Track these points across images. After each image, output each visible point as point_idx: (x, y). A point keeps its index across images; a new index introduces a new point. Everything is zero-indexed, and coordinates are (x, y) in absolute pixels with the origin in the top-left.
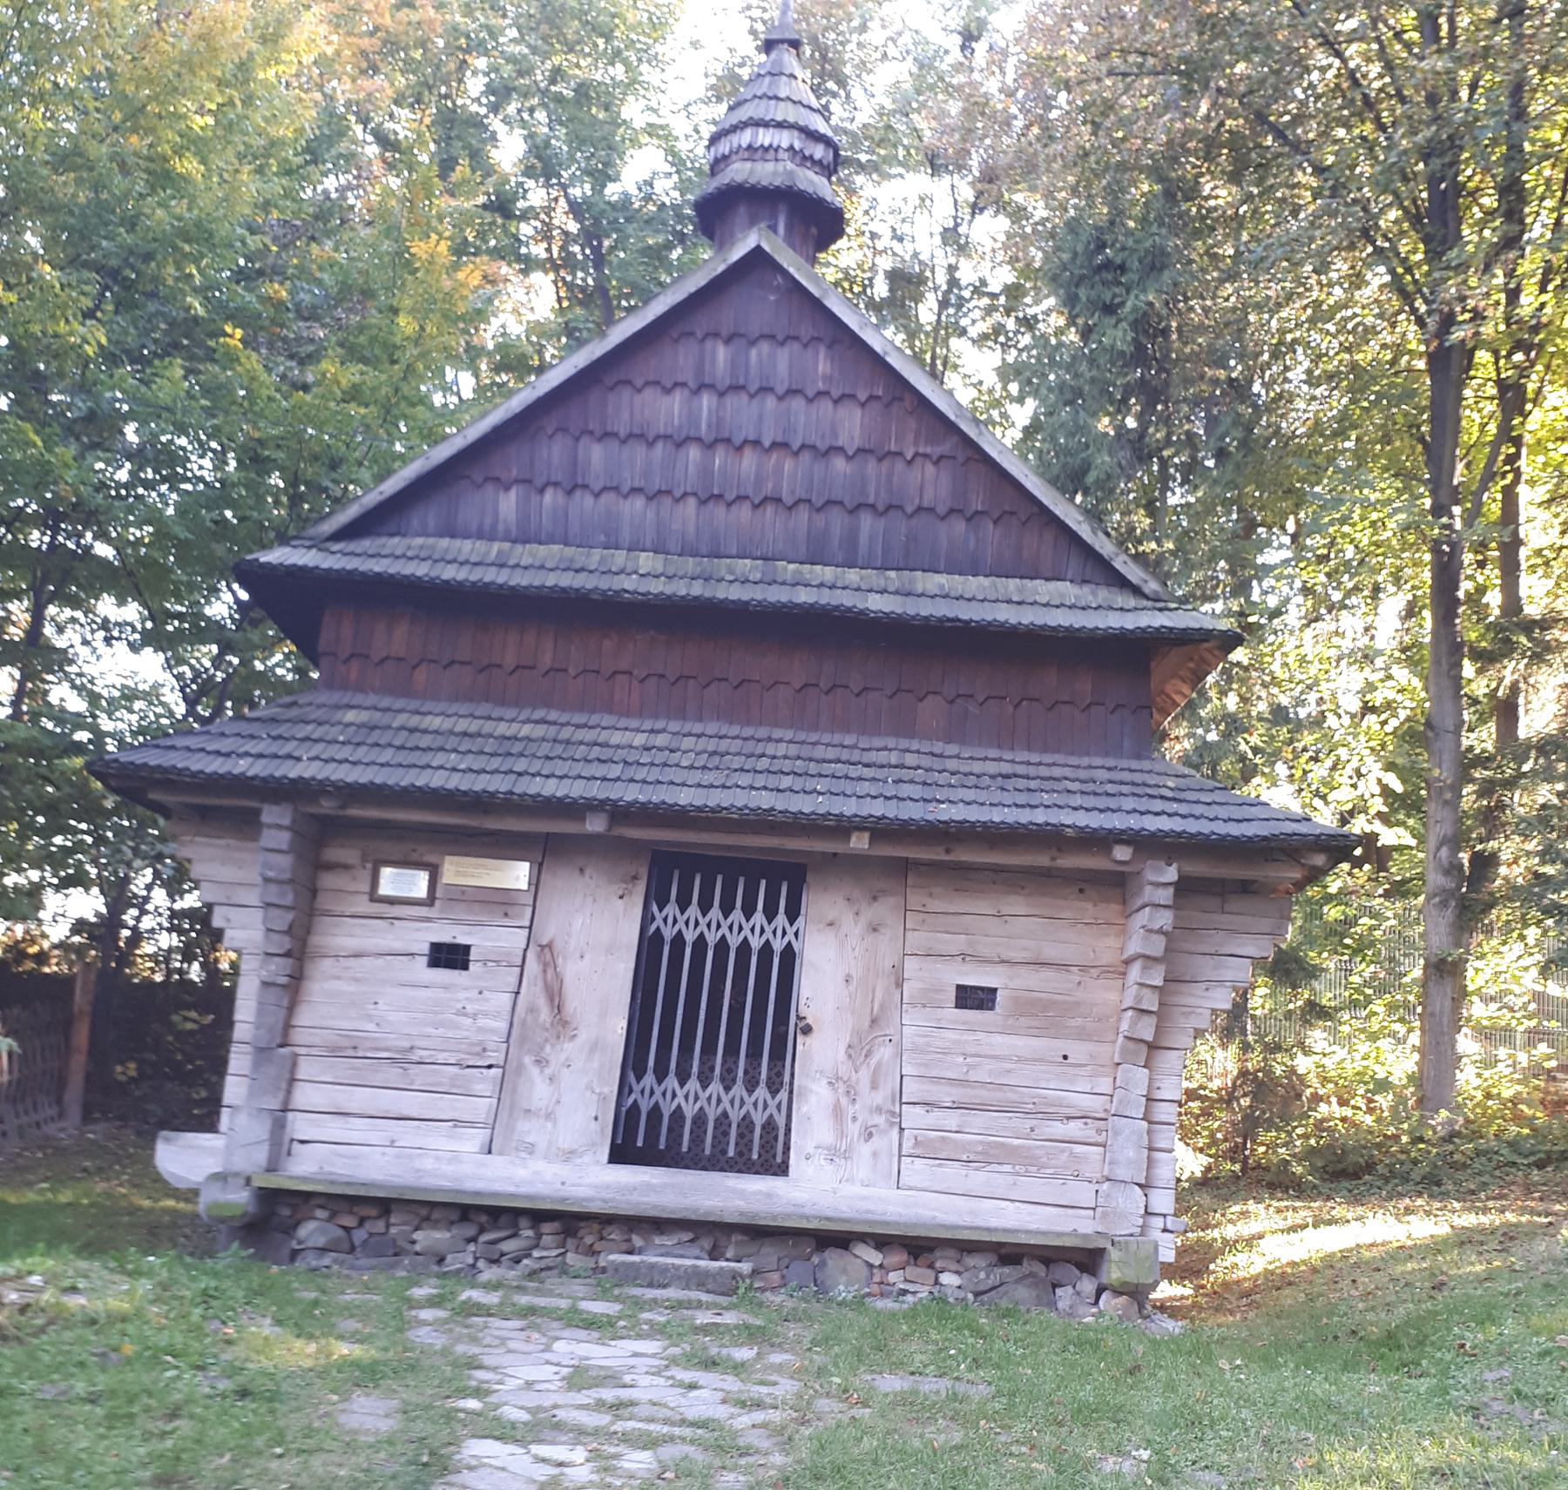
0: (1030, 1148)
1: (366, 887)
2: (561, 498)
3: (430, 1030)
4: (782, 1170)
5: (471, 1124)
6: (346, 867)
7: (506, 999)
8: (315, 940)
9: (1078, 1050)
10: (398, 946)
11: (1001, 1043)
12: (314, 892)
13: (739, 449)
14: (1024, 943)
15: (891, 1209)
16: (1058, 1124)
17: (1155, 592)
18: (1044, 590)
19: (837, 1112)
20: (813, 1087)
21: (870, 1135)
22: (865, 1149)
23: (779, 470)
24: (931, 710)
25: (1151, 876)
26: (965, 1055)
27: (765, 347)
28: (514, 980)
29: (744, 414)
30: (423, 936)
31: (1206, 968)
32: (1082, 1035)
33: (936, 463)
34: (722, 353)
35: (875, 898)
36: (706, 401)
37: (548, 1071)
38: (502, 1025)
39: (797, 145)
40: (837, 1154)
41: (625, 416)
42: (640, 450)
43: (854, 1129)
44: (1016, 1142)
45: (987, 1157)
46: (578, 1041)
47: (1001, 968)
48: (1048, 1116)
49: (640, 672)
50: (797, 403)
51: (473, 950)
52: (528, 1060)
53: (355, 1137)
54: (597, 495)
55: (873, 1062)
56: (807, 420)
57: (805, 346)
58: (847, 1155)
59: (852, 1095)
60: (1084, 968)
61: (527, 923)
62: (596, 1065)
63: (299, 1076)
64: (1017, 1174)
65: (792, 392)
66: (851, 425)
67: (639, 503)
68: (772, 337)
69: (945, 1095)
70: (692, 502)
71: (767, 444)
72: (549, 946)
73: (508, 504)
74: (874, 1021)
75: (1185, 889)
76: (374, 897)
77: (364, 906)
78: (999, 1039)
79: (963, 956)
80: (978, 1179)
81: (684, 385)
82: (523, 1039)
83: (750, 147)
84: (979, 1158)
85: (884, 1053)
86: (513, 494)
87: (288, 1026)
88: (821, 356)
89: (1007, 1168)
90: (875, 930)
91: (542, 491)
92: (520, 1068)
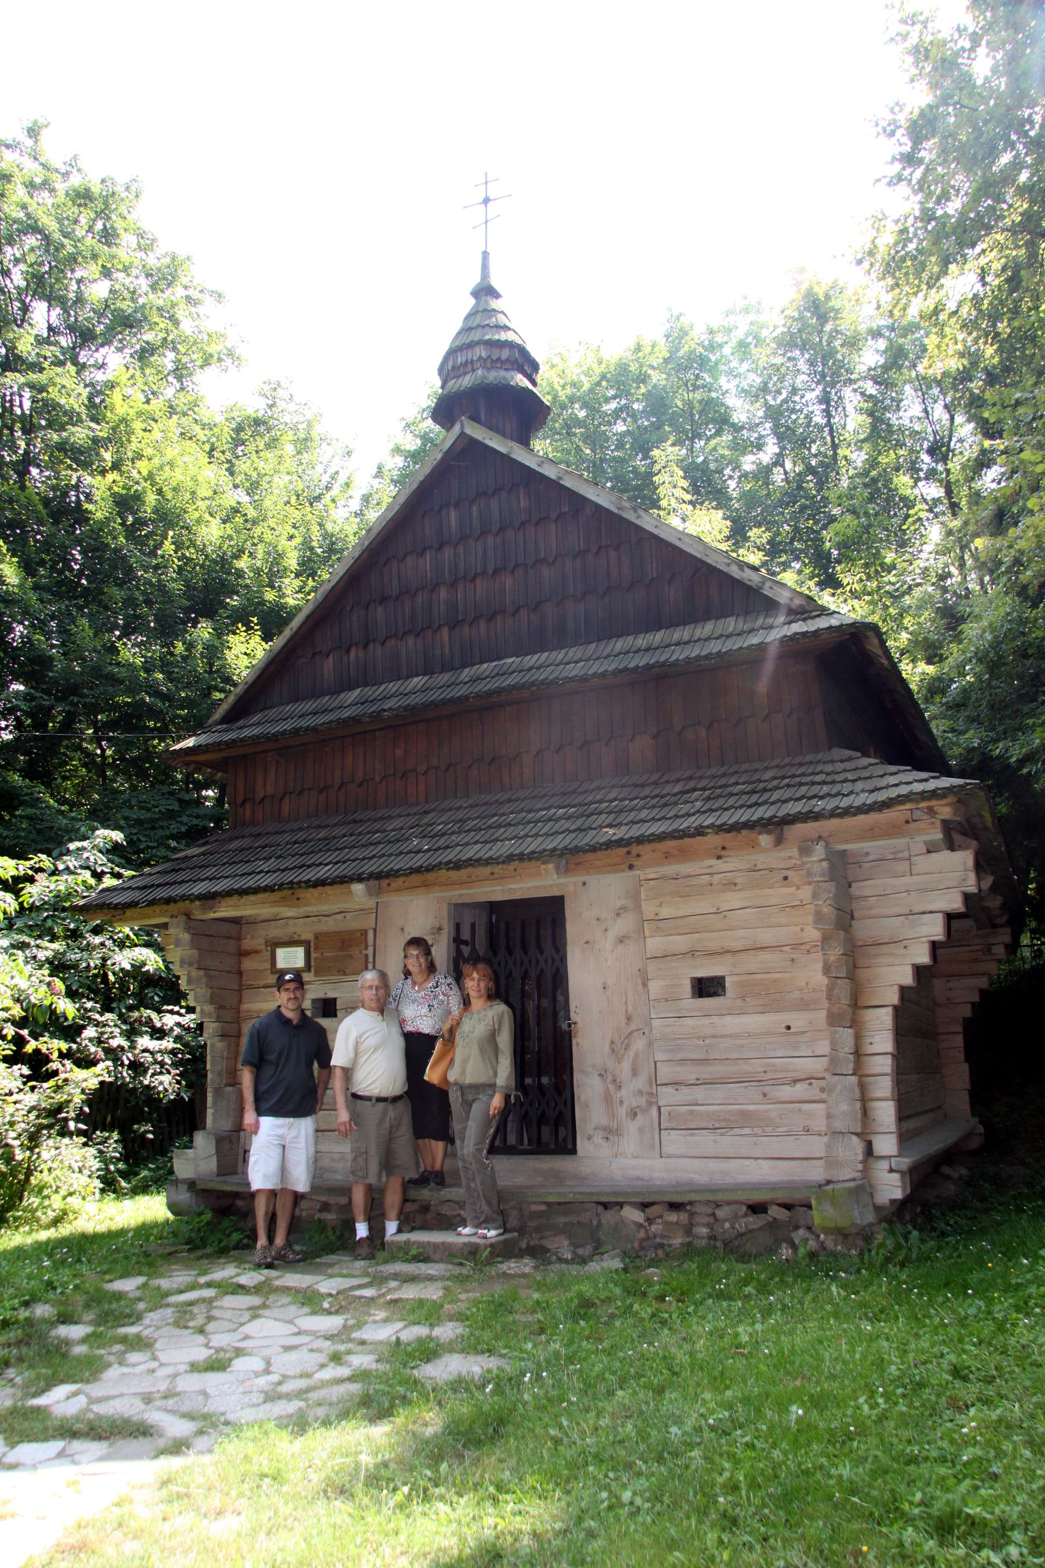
0: (766, 1111)
2: (361, 654)
8: (245, 1007)
9: (798, 1020)
11: (734, 1023)
12: (240, 973)
13: (473, 580)
14: (742, 933)
15: (656, 1174)
16: (787, 1087)
17: (801, 606)
19: (608, 1098)
21: (635, 1114)
22: (632, 1127)
26: (704, 1038)
32: (803, 1006)
33: (617, 548)
35: (618, 915)
39: (484, 355)
41: (395, 582)
43: (622, 1111)
44: (751, 1107)
45: (721, 1125)
47: (728, 958)
49: (421, 769)
51: (338, 1002)
54: (383, 644)
55: (632, 1053)
57: (510, 492)
60: (796, 946)
64: (756, 1135)
69: (690, 1073)
70: (445, 631)
73: (328, 666)
79: (692, 953)
80: (727, 1143)
81: (430, 547)
83: (453, 368)
84: (723, 1124)
85: (639, 1044)
86: (331, 658)
88: (521, 496)
89: (747, 1131)
90: (621, 941)
91: (348, 651)
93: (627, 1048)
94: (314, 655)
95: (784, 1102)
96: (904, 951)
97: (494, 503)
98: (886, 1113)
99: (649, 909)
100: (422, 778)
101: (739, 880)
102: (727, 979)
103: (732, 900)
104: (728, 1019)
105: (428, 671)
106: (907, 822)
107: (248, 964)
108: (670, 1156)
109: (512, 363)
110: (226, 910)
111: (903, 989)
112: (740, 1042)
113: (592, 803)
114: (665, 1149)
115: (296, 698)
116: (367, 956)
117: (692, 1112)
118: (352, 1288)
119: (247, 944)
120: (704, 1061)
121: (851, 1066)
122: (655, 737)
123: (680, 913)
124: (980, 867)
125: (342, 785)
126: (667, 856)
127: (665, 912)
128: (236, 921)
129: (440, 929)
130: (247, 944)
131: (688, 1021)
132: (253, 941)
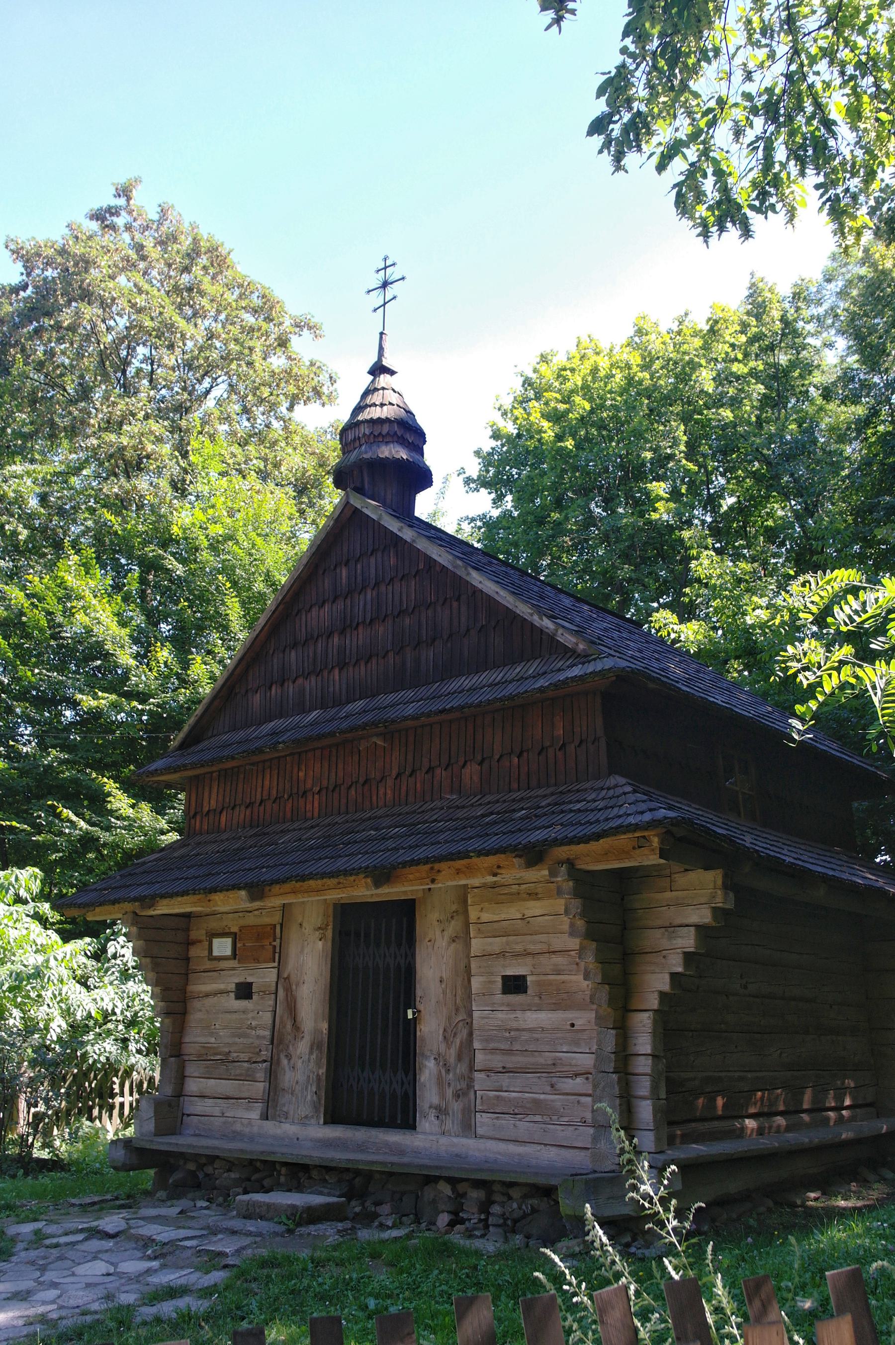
0: (553, 1101)
1: (206, 953)
3: (237, 1040)
4: (413, 1127)
5: (255, 1100)
6: (200, 941)
7: (267, 1017)
8: (191, 988)
12: (188, 959)
13: (357, 628)
16: (570, 1080)
20: (427, 1063)
21: (459, 1096)
26: (510, 1031)
28: (272, 1003)
30: (230, 982)
36: (340, 605)
37: (292, 1062)
38: (267, 1033)
39: (367, 432)
40: (441, 1112)
43: (449, 1092)
44: (542, 1097)
46: (304, 1040)
47: (529, 960)
52: (282, 1056)
53: (208, 1110)
54: (294, 682)
57: (383, 551)
61: (276, 964)
62: (314, 1056)
63: (187, 1074)
70: (336, 671)
71: (368, 621)
72: (288, 978)
76: (211, 958)
77: (208, 965)
79: (502, 954)
80: (523, 1127)
82: (281, 1041)
87: (180, 1043)
89: (538, 1118)
91: (270, 688)
92: (279, 1062)
93: (455, 1034)
94: (247, 691)
95: (567, 1094)
96: (663, 961)
98: (645, 1111)
99: (473, 914)
100: (316, 797)
101: (539, 890)
102: (529, 979)
103: (534, 908)
104: (528, 1013)
105: (323, 706)
106: (634, 848)
107: (195, 952)
108: (482, 1137)
109: (392, 436)
110: (164, 908)
111: (663, 995)
112: (536, 1036)
113: (419, 823)
114: (480, 1131)
115: (234, 729)
116: (275, 947)
117: (498, 1097)
118: (180, 1240)
119: (194, 935)
120: (509, 1052)
121: (612, 1065)
122: (481, 764)
123: (496, 918)
124: (729, 885)
125: (262, 801)
126: (458, 871)
127: (486, 917)
128: (188, 916)
129: (327, 925)
130: (194, 935)
131: (500, 1015)
132: (197, 933)
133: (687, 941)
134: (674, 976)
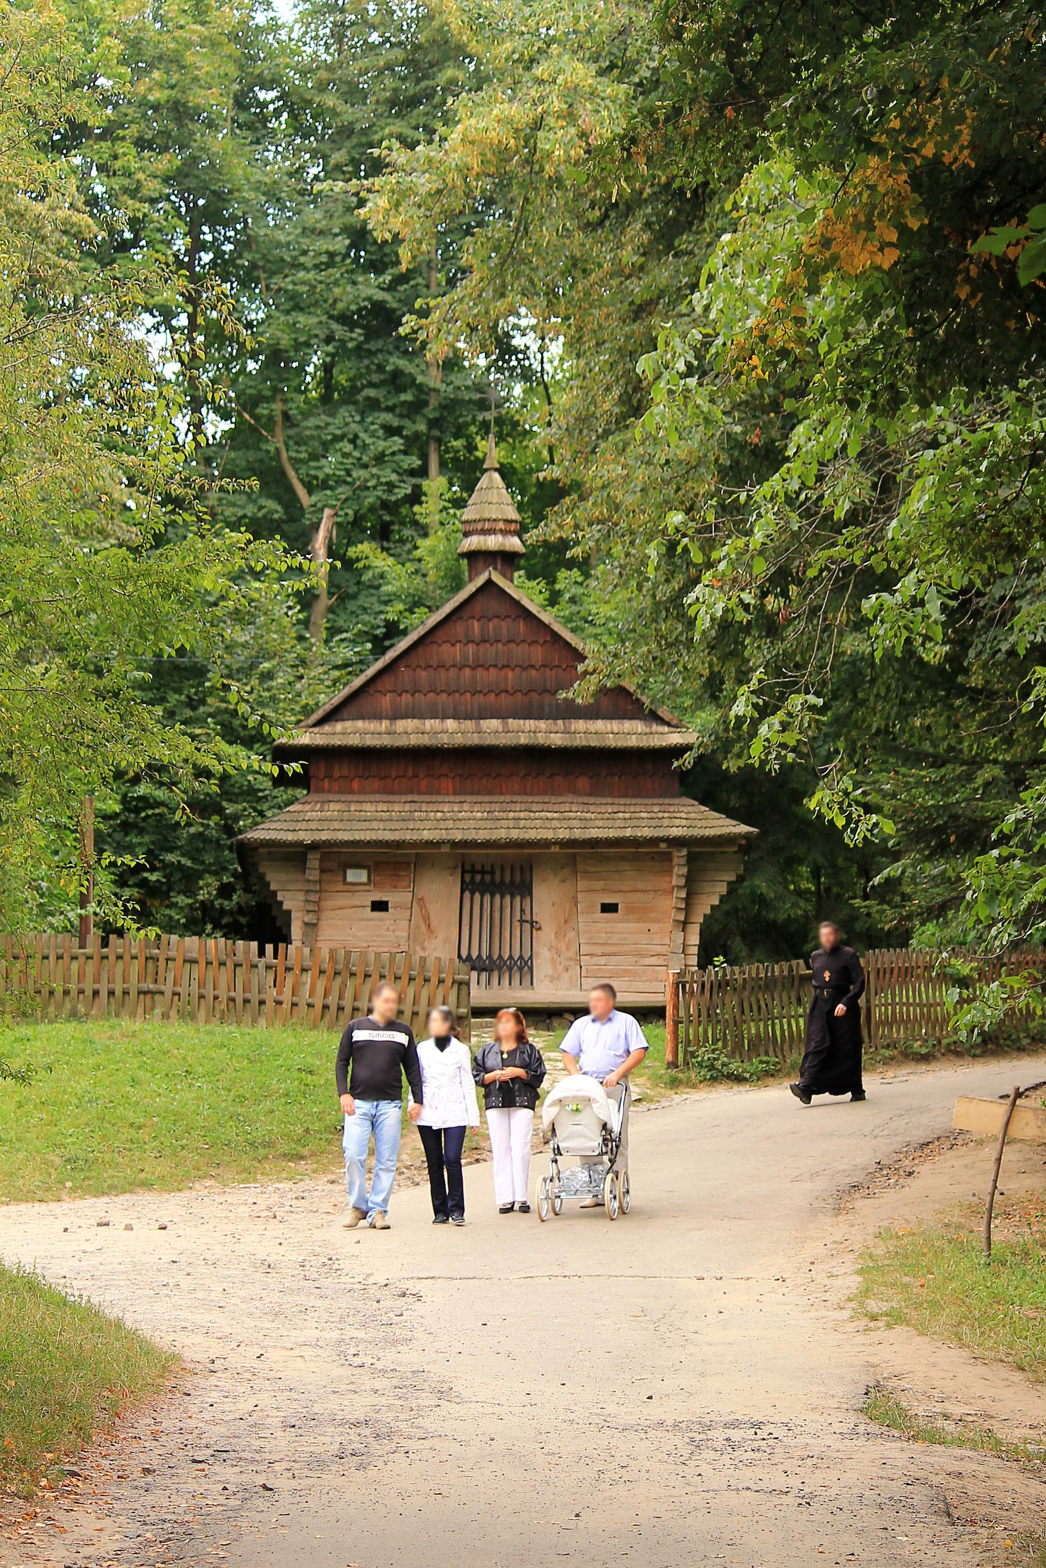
9: (654, 927)
10: (357, 903)
13: (487, 669)
18: (628, 725)
19: (553, 962)
23: (506, 678)
24: (583, 782)
25: (676, 854)
27: (495, 621)
29: (490, 652)
31: (707, 887)
32: (656, 920)
34: (477, 625)
36: (471, 648)
40: (553, 979)
41: (435, 658)
42: (443, 673)
43: (560, 968)
48: (643, 956)
50: (513, 646)
56: (519, 652)
58: (558, 978)
59: (558, 953)
65: (509, 641)
66: (537, 654)
67: (444, 696)
68: (498, 617)
69: (598, 950)
70: (468, 695)
73: (386, 701)
74: (566, 922)
75: (691, 859)
77: (341, 887)
78: (620, 925)
79: (603, 890)
85: (572, 935)
97: (504, 624)
133: (723, 889)
134: (712, 907)
